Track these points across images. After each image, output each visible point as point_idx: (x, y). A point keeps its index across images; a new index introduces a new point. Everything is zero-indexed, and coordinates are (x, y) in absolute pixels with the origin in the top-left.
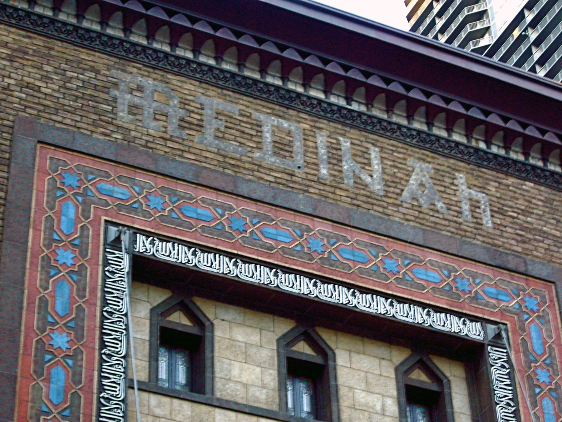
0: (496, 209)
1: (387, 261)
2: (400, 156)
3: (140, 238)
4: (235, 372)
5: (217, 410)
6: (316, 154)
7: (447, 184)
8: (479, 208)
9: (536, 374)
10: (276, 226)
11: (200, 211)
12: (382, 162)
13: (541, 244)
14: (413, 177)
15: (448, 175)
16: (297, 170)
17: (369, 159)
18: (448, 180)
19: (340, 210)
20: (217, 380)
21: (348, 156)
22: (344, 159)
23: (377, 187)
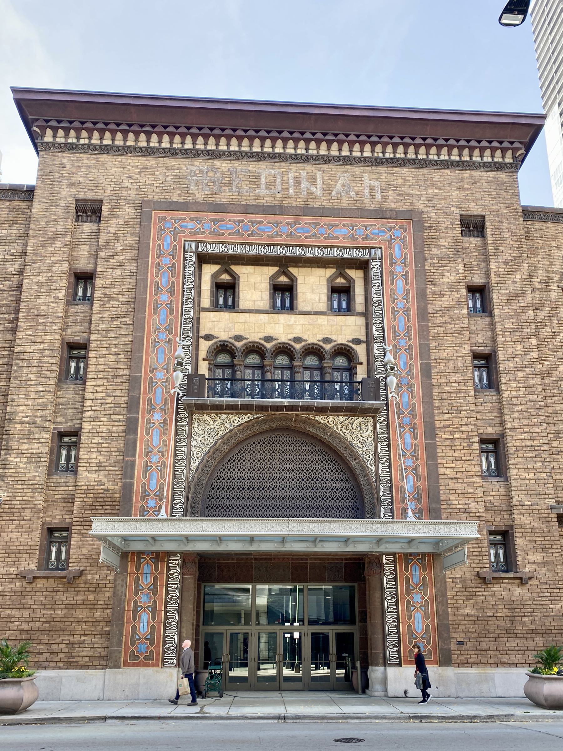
3: (200, 245)
11: (228, 226)
12: (323, 179)
22: (302, 182)
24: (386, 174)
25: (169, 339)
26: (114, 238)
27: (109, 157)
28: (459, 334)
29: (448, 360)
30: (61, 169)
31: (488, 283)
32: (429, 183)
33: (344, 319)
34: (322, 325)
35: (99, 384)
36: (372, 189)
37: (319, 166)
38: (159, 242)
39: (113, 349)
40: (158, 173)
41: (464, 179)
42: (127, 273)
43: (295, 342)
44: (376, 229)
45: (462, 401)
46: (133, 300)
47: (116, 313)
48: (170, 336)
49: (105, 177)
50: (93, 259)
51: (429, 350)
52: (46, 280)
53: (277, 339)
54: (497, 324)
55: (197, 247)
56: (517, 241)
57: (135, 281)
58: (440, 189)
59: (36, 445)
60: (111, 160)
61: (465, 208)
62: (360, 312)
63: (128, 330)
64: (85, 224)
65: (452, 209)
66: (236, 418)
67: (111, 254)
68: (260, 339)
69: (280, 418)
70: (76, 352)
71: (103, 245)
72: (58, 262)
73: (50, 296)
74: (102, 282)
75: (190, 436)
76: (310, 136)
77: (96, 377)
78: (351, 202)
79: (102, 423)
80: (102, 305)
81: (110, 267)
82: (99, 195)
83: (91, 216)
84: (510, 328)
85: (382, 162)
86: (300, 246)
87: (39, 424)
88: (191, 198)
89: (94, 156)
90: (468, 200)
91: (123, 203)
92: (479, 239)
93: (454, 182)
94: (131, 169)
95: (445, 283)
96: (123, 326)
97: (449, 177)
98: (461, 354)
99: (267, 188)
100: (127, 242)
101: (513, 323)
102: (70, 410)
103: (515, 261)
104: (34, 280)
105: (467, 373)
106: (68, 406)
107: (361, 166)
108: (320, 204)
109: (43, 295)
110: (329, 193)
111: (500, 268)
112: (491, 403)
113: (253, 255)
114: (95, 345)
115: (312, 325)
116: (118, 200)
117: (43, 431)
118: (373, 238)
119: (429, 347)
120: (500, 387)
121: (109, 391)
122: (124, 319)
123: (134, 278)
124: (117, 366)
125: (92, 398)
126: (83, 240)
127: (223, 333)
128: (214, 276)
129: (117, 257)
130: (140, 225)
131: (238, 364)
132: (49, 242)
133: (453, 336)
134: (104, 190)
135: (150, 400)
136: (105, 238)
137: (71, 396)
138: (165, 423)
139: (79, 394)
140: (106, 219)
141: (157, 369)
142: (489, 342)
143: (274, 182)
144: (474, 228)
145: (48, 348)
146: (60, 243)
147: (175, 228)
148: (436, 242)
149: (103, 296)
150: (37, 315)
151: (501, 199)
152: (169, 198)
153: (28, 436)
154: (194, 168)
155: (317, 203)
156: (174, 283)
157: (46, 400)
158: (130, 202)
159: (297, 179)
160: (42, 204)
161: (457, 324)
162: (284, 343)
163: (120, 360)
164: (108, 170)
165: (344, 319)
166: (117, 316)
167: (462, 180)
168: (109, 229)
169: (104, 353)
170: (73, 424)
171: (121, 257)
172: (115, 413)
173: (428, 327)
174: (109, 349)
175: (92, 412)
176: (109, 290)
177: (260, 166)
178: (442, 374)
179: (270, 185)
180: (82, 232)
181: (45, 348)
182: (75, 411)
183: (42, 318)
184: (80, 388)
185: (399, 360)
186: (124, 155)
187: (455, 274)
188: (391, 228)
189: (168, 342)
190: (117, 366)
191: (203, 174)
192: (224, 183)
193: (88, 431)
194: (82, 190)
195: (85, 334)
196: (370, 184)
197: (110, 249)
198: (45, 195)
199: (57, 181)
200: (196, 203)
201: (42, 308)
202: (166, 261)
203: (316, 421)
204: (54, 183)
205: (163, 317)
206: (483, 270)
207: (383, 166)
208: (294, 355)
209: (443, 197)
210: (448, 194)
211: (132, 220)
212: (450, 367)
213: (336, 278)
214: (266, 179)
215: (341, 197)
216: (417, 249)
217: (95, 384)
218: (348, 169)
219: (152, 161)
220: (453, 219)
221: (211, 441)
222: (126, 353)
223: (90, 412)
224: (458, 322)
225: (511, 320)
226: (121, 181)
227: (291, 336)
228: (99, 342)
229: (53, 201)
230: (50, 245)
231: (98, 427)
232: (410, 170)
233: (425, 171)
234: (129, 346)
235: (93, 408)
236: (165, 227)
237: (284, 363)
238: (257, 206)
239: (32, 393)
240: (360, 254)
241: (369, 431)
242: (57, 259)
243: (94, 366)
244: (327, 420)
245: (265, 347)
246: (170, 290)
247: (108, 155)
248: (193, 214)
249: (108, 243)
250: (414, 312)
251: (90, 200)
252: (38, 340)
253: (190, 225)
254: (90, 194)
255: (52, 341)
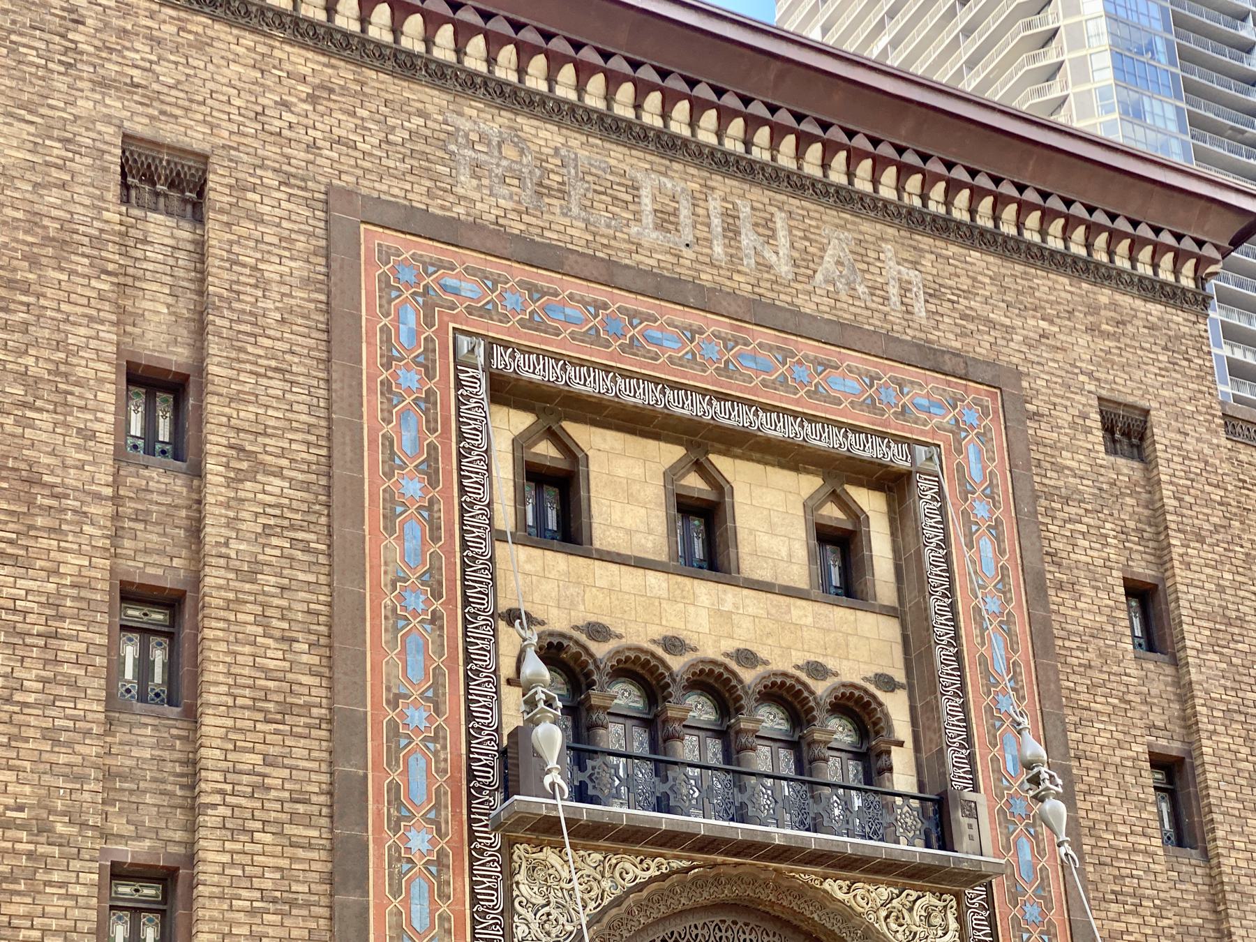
0: (931, 291)
1: (796, 368)
2: (813, 223)
3: (498, 350)
4: (616, 516)
5: (597, 562)
6: (709, 226)
7: (871, 260)
8: (910, 290)
9: (973, 509)
10: (661, 328)
11: (568, 311)
12: (790, 232)
13: (986, 337)
14: (830, 252)
15: (872, 247)
16: (684, 249)
17: (773, 230)
18: (872, 254)
19: (740, 302)
20: (594, 525)
21: (749, 226)
22: (743, 231)
23: (784, 269)
24: (933, 257)
25: (434, 612)
26: (253, 281)
27: (217, 26)
28: (1122, 700)
29: (1105, 764)
30: (71, 25)
31: (1163, 580)
32: (1028, 300)
33: (852, 618)
34: (801, 626)
35: (239, 724)
36: (905, 288)
37: (778, 197)
38: (385, 321)
39: (275, 623)
40: (365, 114)
41: (1100, 308)
42: (299, 395)
43: (739, 663)
44: (923, 397)
45: (1141, 873)
46: (323, 481)
47: (278, 512)
48: (437, 605)
49: (210, 85)
50: (185, 333)
51: (1065, 731)
52: (49, 372)
53: (695, 650)
54: (1196, 686)
55: (489, 355)
56: (1217, 486)
57: (323, 423)
58: (1052, 322)
59: (56, 905)
60: (222, 36)
61: (1106, 382)
62: (886, 603)
63: (314, 568)
64: (152, 216)
65: (1082, 378)
66: (628, 866)
67: (248, 328)
68: (654, 641)
69: (739, 877)
70: (136, 613)
71: (220, 297)
72: (85, 321)
73: (66, 425)
74: (227, 410)
75: (509, 910)
76: (765, 113)
77: (230, 702)
78: (858, 311)
79: (258, 848)
80: (234, 481)
81: (248, 367)
82: (196, 138)
83: (166, 196)
84: (1221, 700)
85: (923, 220)
86: (750, 403)
87: (61, 836)
88: (461, 210)
89: (173, 13)
90: (1113, 363)
91: (271, 180)
92: (1136, 465)
93: (1080, 312)
94: (285, 81)
95: (1080, 565)
96: (299, 555)
97: (1069, 296)
98: (1130, 754)
99: (659, 227)
100: (293, 301)
101: (1225, 688)
102: (148, 799)
103: (1216, 536)
104: (9, 366)
105: (1146, 802)
106: (142, 785)
107: (876, 220)
108: (789, 299)
109: (44, 420)
110: (809, 277)
111: (1188, 546)
112: (1196, 885)
113: (635, 406)
114: (221, 603)
115: (777, 621)
116: (255, 166)
117: (78, 857)
118: (918, 418)
119: (1063, 723)
120: (1210, 846)
121: (271, 750)
122: (300, 535)
123: (323, 413)
124: (289, 676)
125: (224, 765)
126: (150, 266)
127: (554, 612)
128: (520, 443)
129: (268, 342)
130: (327, 257)
131: (599, 707)
132: (50, 251)
133: (1108, 703)
134: (212, 126)
135: (394, 789)
136: (225, 275)
137: (147, 754)
138: (440, 862)
139: (173, 748)
140: (225, 218)
141: (406, 697)
142: (1178, 730)
143: (675, 215)
144: (1123, 434)
145: (74, 592)
146: (86, 261)
147: (426, 287)
148: (1053, 456)
149: (234, 452)
150: (30, 482)
151: (1179, 376)
152: (402, 194)
153: (28, 873)
154: (466, 125)
155: (782, 297)
156: (436, 448)
157: (79, 760)
158: (292, 181)
159: (730, 220)
160: (16, 123)
161: (1115, 674)
162: (713, 662)
163: (298, 658)
164: (218, 66)
165: (852, 618)
166: (279, 521)
167: (1094, 309)
168: (236, 249)
169: (251, 629)
170: (159, 844)
171: (278, 344)
172: (293, 818)
173: (1057, 672)
174: (262, 620)
175: (228, 812)
176: (251, 437)
177: (634, 161)
178: (1095, 799)
179: (666, 221)
180: (145, 241)
181: (63, 591)
182: (165, 801)
183: (47, 492)
184: (174, 732)
185: (1003, 749)
186: (265, 35)
187: (1098, 546)
188: (955, 400)
189: (432, 622)
190: (289, 676)
191: (489, 145)
192: (549, 188)
193: (219, 869)
194: (140, 109)
195: (176, 562)
196: (899, 272)
197: (244, 312)
198: (25, 97)
199: (60, 62)
200: (476, 225)
201: (45, 460)
202: (410, 379)
203: (826, 892)
204: (51, 65)
205: (412, 544)
206: (1151, 544)
207: (923, 234)
208: (739, 698)
209: (1059, 345)
210: (1069, 339)
211: (303, 238)
212: (1110, 783)
213: (821, 505)
214: (654, 200)
215: (837, 293)
216: (1017, 466)
217: (230, 723)
218: (846, 221)
219: (343, 73)
220: (1084, 405)
221: (569, 928)
222: (314, 638)
223: (222, 810)
224: (1115, 669)
225: (1222, 681)
226: (259, 109)
227: (729, 645)
228: (231, 596)
229: (51, 122)
230: (53, 263)
231: (247, 859)
232: (984, 257)
233: (1017, 267)
234: (322, 619)
235: (229, 799)
236: (398, 280)
237: (705, 717)
238: (638, 271)
239: (31, 733)
240: (890, 454)
241: (950, 934)
242: (79, 310)
243: (221, 668)
244: (852, 894)
245: (668, 668)
246: (424, 467)
247: (215, 19)
248: (474, 259)
249: (238, 293)
250: (1021, 627)
251: (169, 147)
252: (39, 564)
253: (469, 288)
254: (168, 127)
255: (85, 572)
